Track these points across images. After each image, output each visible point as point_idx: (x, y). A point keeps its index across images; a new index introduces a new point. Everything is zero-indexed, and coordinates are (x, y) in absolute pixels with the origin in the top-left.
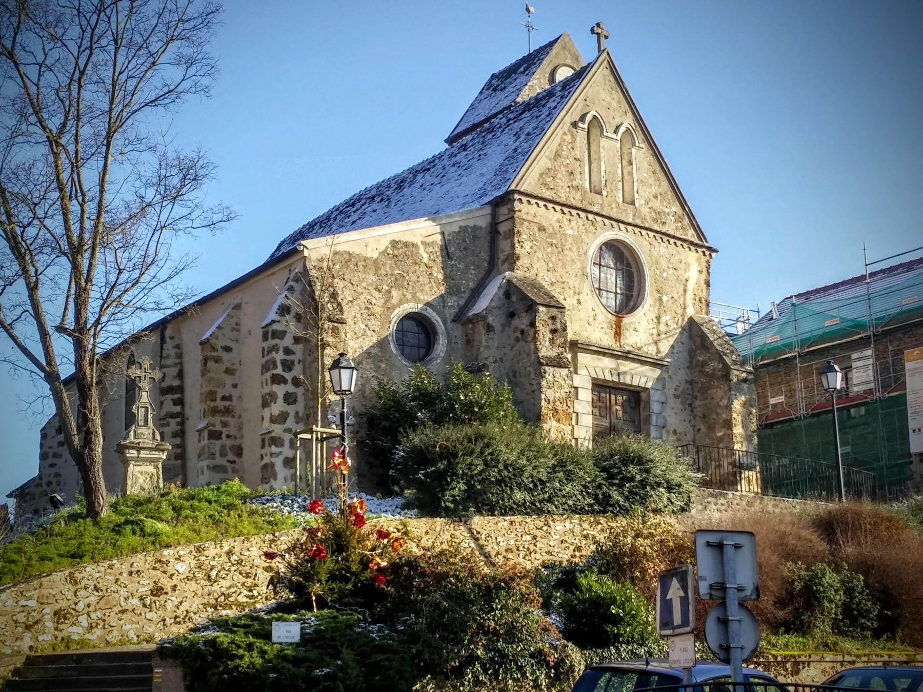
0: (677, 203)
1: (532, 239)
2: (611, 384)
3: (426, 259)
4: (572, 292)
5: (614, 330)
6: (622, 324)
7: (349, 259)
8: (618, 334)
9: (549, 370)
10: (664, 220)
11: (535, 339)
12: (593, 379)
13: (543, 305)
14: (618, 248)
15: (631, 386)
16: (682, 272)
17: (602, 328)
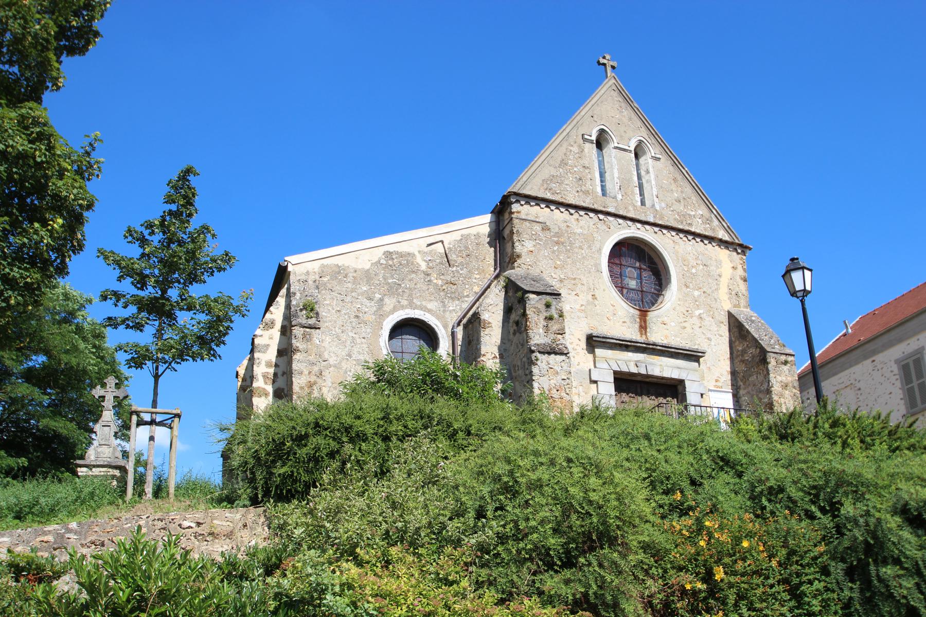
0: (703, 207)
1: (534, 238)
2: (639, 378)
3: (423, 266)
4: (585, 288)
5: (638, 324)
6: (648, 318)
7: (339, 273)
8: (643, 328)
10: (689, 222)
12: (615, 373)
14: (638, 247)
15: (663, 378)
16: (713, 268)
17: (624, 322)
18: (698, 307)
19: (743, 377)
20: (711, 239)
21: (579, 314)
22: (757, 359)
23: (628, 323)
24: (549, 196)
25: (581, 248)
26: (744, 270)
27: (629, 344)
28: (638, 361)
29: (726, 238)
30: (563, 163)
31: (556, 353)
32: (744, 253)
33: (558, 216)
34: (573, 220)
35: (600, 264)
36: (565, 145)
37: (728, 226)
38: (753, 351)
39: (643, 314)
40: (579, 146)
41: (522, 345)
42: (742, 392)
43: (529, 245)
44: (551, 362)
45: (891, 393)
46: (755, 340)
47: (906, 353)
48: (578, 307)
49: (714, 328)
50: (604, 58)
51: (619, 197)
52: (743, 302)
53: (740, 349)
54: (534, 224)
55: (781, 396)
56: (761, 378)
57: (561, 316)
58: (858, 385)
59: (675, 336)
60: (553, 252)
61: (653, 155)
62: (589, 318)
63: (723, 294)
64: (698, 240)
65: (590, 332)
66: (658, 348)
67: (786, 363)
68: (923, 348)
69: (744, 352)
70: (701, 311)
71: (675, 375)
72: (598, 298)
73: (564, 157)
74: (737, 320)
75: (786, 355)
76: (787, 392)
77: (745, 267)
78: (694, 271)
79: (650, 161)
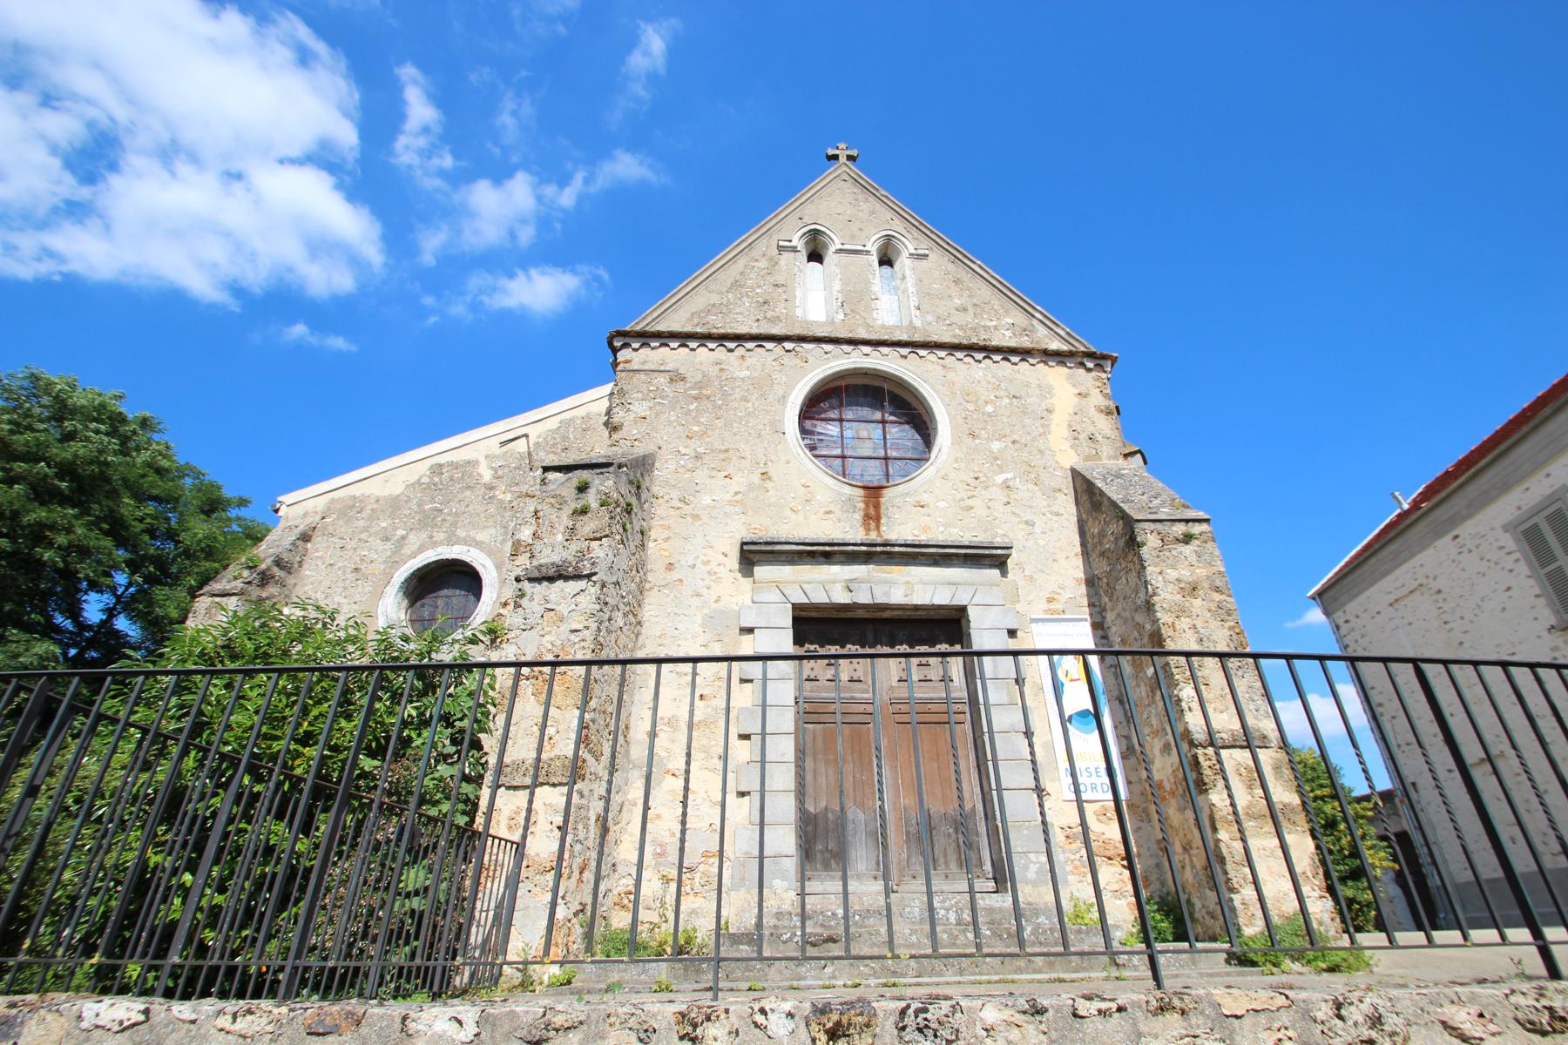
2: (861, 614)
5: (862, 513)
6: (882, 500)
7: (352, 508)
8: (873, 516)
12: (795, 607)
15: (916, 608)
18: (1001, 469)
19: (1108, 584)
21: (728, 509)
22: (1122, 542)
23: (838, 513)
25: (745, 399)
26: (1106, 396)
27: (827, 548)
28: (851, 581)
29: (1055, 345)
31: (566, 578)
32: (1099, 367)
33: (705, 356)
34: (732, 359)
35: (781, 421)
36: (742, 262)
37: (1068, 333)
43: (640, 408)
44: (552, 597)
45: (1509, 589)
46: (1114, 504)
47: (1524, 508)
48: (728, 497)
49: (1041, 501)
54: (656, 374)
58: (1435, 585)
59: (948, 525)
60: (688, 412)
61: (913, 251)
62: (750, 513)
64: (997, 358)
65: (749, 537)
66: (897, 549)
67: (1187, 539)
69: (1102, 534)
70: (1009, 476)
71: (942, 598)
72: (774, 477)
73: (738, 277)
74: (1084, 477)
75: (1187, 521)
76: (1198, 602)
77: (1108, 391)
78: (989, 409)
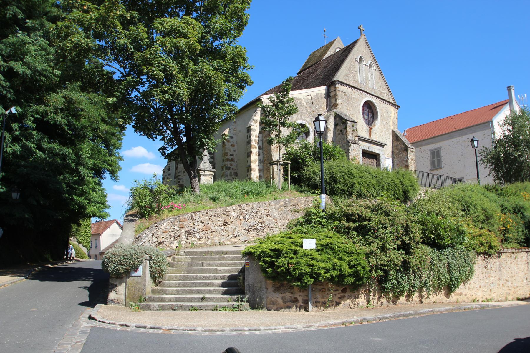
0: (387, 90)
1: (342, 98)
2: (368, 152)
3: (305, 105)
8: (370, 134)
9: (352, 145)
11: (346, 134)
12: (363, 150)
13: (349, 121)
15: (374, 153)
20: (389, 103)
24: (345, 82)
25: (355, 103)
30: (349, 69)
31: (356, 144)
33: (348, 90)
38: (401, 146)
39: (371, 129)
40: (354, 63)
41: (344, 139)
42: (395, 159)
46: (404, 143)
50: (361, 26)
51: (365, 84)
52: (396, 127)
53: (396, 144)
55: (411, 163)
56: (404, 156)
57: (357, 130)
63: (391, 123)
68: (441, 147)
69: (397, 145)
79: (373, 70)
